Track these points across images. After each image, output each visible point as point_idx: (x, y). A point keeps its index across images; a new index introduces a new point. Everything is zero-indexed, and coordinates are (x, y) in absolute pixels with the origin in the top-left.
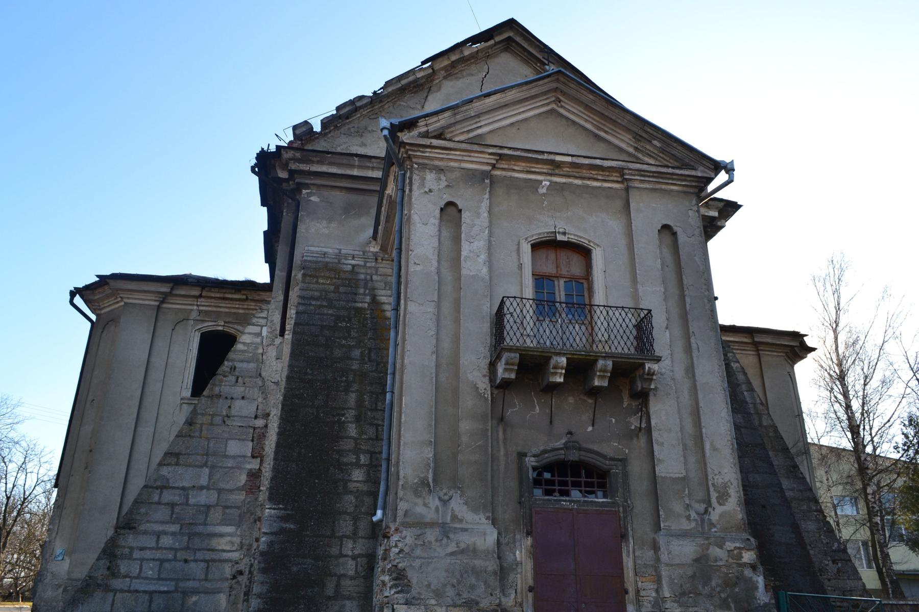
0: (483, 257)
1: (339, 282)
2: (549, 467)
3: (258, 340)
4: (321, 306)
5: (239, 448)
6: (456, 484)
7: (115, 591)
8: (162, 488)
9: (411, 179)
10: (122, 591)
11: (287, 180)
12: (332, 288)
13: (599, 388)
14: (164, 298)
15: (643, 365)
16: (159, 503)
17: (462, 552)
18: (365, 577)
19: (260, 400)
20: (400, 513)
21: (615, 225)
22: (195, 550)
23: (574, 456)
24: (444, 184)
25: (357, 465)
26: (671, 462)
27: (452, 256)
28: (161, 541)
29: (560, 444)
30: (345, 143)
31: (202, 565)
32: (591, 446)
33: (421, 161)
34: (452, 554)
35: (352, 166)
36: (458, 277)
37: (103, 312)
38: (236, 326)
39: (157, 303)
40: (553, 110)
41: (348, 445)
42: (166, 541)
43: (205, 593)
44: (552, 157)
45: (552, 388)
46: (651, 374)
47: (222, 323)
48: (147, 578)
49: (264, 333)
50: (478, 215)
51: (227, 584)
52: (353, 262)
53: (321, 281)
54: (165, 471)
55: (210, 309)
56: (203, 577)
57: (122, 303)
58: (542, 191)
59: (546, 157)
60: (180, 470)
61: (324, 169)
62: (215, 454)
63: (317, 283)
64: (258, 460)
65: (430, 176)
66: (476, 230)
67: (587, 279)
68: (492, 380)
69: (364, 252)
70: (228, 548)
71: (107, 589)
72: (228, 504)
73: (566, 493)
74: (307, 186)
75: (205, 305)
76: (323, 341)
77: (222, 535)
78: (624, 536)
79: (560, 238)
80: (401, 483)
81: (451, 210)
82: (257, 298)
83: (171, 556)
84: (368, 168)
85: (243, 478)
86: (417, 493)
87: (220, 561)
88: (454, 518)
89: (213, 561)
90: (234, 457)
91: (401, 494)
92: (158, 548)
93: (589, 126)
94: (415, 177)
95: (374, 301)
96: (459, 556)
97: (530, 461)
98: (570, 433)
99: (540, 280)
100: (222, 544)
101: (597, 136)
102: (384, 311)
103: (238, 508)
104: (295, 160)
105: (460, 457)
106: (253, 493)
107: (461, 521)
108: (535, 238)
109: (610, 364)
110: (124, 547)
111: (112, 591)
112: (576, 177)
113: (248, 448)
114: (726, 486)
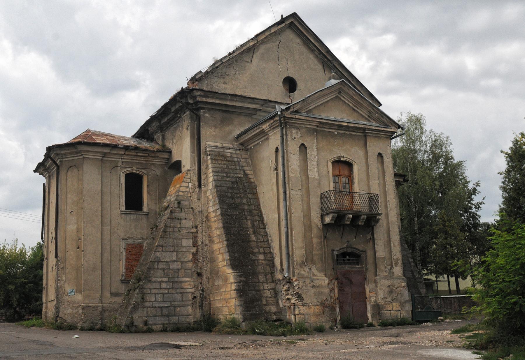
0: (316, 169)
3: (188, 190)
4: (224, 176)
5: (187, 242)
6: (313, 262)
7: (147, 307)
8: (159, 262)
9: (286, 132)
10: (149, 307)
11: (192, 104)
12: (225, 166)
13: (359, 225)
14: (105, 155)
15: (375, 217)
16: (158, 269)
18: (275, 297)
20: (296, 274)
21: (361, 153)
22: (176, 289)
23: (349, 250)
24: (300, 135)
25: (259, 253)
26: (381, 252)
27: (305, 170)
29: (345, 246)
30: (216, 82)
31: (180, 295)
32: (354, 246)
33: (290, 124)
35: (226, 100)
37: (64, 160)
38: (142, 171)
39: (101, 158)
40: (337, 96)
42: (164, 285)
45: (345, 226)
46: (379, 220)
47: (135, 169)
49: (190, 186)
50: (313, 150)
51: (190, 302)
53: (220, 162)
54: (158, 254)
57: (81, 157)
59: (338, 123)
60: (164, 253)
61: (213, 101)
62: (177, 246)
63: (218, 163)
64: (196, 248)
65: (294, 131)
66: (313, 156)
67: (350, 176)
71: (144, 307)
72: (186, 268)
74: (203, 108)
75: (126, 159)
76: (230, 195)
77: (186, 282)
78: (365, 279)
79: (342, 159)
80: (295, 263)
81: (303, 147)
83: (166, 291)
84: (233, 100)
85: (190, 257)
86: (301, 267)
87: (187, 293)
88: (314, 275)
89: (184, 293)
90: (186, 247)
91: (295, 267)
92: (161, 289)
93: (351, 105)
94: (288, 132)
95: (245, 174)
97: (336, 253)
98: (348, 242)
100: (186, 285)
101: (354, 109)
102: (250, 178)
103: (190, 269)
104: (201, 96)
105: (314, 253)
106: (196, 263)
107: (316, 276)
109: (366, 217)
110: (147, 289)
111: (145, 307)
114: (397, 259)
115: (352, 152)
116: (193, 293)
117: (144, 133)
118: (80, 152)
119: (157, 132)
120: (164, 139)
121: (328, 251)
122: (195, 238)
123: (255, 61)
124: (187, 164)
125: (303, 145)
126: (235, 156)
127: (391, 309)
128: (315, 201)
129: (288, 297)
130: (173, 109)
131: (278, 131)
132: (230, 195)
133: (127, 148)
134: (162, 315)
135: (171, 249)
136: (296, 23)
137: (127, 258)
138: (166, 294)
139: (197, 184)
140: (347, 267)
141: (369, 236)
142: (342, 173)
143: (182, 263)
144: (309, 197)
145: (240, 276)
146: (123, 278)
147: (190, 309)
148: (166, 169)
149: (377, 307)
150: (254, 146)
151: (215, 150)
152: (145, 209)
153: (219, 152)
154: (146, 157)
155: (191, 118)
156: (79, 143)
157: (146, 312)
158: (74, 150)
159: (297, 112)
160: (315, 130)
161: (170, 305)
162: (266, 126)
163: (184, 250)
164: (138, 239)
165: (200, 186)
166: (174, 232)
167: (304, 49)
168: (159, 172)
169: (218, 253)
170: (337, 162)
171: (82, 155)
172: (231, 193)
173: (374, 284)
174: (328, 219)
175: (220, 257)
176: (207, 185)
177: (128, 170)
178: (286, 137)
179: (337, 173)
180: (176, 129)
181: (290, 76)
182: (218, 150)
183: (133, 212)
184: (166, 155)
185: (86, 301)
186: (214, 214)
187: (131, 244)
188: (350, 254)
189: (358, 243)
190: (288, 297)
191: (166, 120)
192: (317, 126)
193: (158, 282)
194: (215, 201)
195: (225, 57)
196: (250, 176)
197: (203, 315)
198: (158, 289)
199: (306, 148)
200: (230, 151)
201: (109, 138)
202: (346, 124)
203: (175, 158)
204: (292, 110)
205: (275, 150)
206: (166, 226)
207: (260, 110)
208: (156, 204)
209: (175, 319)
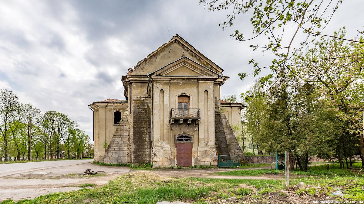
2: (180, 137)
3: (127, 115)
5: (126, 134)
8: (114, 141)
12: (140, 104)
14: (107, 106)
17: (165, 150)
23: (184, 135)
25: (147, 137)
29: (182, 133)
36: (164, 105)
42: (116, 149)
49: (128, 113)
52: (143, 98)
53: (137, 103)
54: (114, 139)
58: (180, 85)
65: (157, 84)
68: (170, 123)
73: (183, 141)
79: (184, 95)
81: (162, 91)
88: (163, 145)
95: (148, 107)
97: (176, 136)
108: (178, 96)
109: (191, 119)
115: (190, 91)
121: (172, 135)
128: (167, 114)
141: (196, 129)
142: (184, 101)
149: (197, 160)
172: (140, 115)
177: (116, 111)
185: (100, 155)
188: (185, 137)
189: (188, 131)
193: (114, 148)
209: (120, 161)
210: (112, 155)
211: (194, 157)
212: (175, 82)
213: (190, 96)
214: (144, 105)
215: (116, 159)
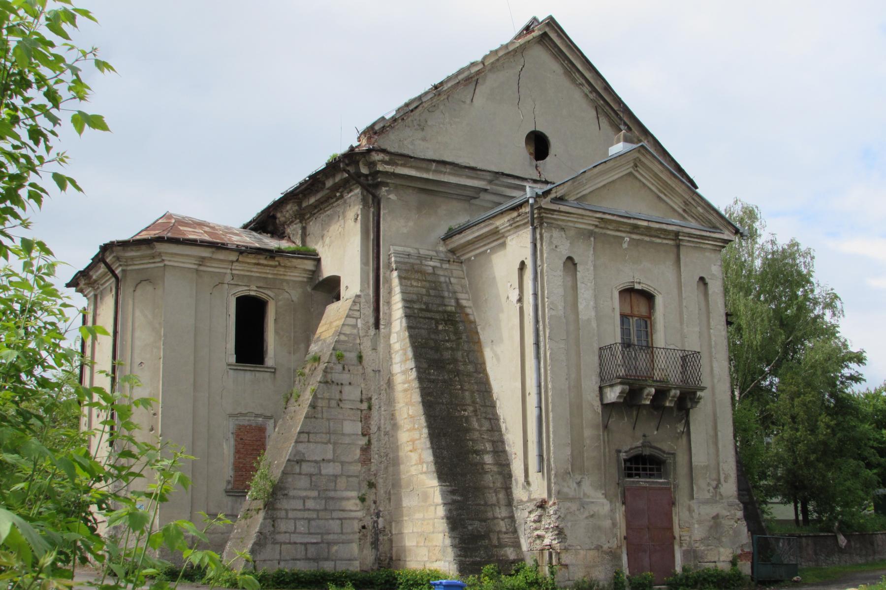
1: (427, 284)
3: (355, 331)
5: (352, 427)
6: (582, 470)
7: (281, 544)
10: (285, 543)
11: (366, 176)
12: (424, 291)
13: (665, 408)
15: (695, 393)
16: (300, 474)
17: (592, 516)
19: (363, 385)
23: (647, 452)
26: (701, 455)
28: (307, 504)
29: (639, 443)
31: (338, 522)
32: (656, 445)
33: (549, 221)
34: (587, 518)
35: (427, 170)
37: (129, 268)
39: (195, 267)
40: (630, 174)
41: (476, 435)
42: (310, 504)
43: (343, 543)
44: (635, 222)
45: (640, 407)
46: (700, 398)
47: (255, 288)
48: (300, 533)
49: (359, 325)
51: (357, 536)
52: (431, 263)
53: (415, 284)
54: (301, 447)
55: (242, 273)
56: (339, 531)
57: (161, 265)
58: (625, 246)
59: (632, 221)
60: (312, 446)
63: (412, 286)
64: (367, 438)
65: (556, 233)
67: (650, 318)
69: (436, 252)
70: (354, 508)
71: (275, 542)
72: (350, 474)
73: (639, 475)
74: (386, 184)
77: (348, 499)
78: (673, 504)
79: (637, 287)
81: (570, 264)
82: (289, 264)
83: (315, 516)
84: (441, 172)
87: (350, 519)
88: (585, 494)
89: (345, 519)
90: (349, 435)
92: (305, 510)
93: (653, 188)
96: (591, 519)
97: (623, 456)
98: (644, 436)
99: (624, 317)
101: (659, 197)
103: (357, 477)
104: (383, 162)
107: (588, 497)
108: (622, 287)
109: (678, 392)
111: (277, 543)
112: (647, 235)
113: (358, 428)
115: (653, 273)
116: (361, 520)
117: (266, 222)
118: (160, 255)
119: (292, 222)
120: (304, 235)
121: (609, 451)
122: (366, 419)
123: (479, 101)
124: (352, 286)
125: (570, 259)
126: (440, 272)
127: (716, 559)
128: (591, 361)
129: (538, 532)
130: (329, 183)
131: (526, 235)
132: (432, 344)
133: (243, 251)
134: (307, 559)
135: (325, 438)
136: (553, 36)
137: (237, 452)
138: (313, 519)
139: (372, 320)
140: (642, 482)
141: (681, 428)
143: (342, 465)
144: (578, 354)
145: (453, 492)
146: (230, 487)
147: (355, 548)
148: (309, 289)
150: (475, 256)
151: (406, 260)
152: (270, 361)
153: (413, 265)
154: (275, 267)
155: (364, 201)
156: (160, 240)
157: (278, 551)
158: (149, 252)
159: (560, 199)
160: (591, 234)
161: (319, 540)
162: (502, 223)
163: (347, 440)
164: (257, 416)
165: (377, 325)
166: (329, 407)
167: (565, 82)
168: (295, 294)
169: (410, 448)
170: (629, 292)
171: (163, 260)
173: (687, 513)
174: (613, 395)
175: (414, 457)
176: (389, 324)
177: (242, 291)
178: (542, 245)
179: (627, 311)
180: (330, 218)
181: (537, 129)
182: (412, 261)
183: (248, 367)
184: (309, 265)
186: (403, 377)
187: (243, 426)
189: (661, 438)
190: (538, 532)
191: (312, 200)
192: (596, 226)
193: (300, 498)
194: (405, 354)
195: (426, 93)
196: (469, 311)
197: (378, 560)
198: (300, 510)
199: (575, 265)
200: (431, 263)
201: (207, 229)
202: (645, 224)
203: (327, 271)
204: (553, 195)
205: (518, 266)
206: (315, 397)
207: (486, 190)
208: (290, 353)
210: (294, 533)
211: (681, 546)
212: (609, 232)
213: (655, 293)
214: (443, 297)
215: (309, 555)
